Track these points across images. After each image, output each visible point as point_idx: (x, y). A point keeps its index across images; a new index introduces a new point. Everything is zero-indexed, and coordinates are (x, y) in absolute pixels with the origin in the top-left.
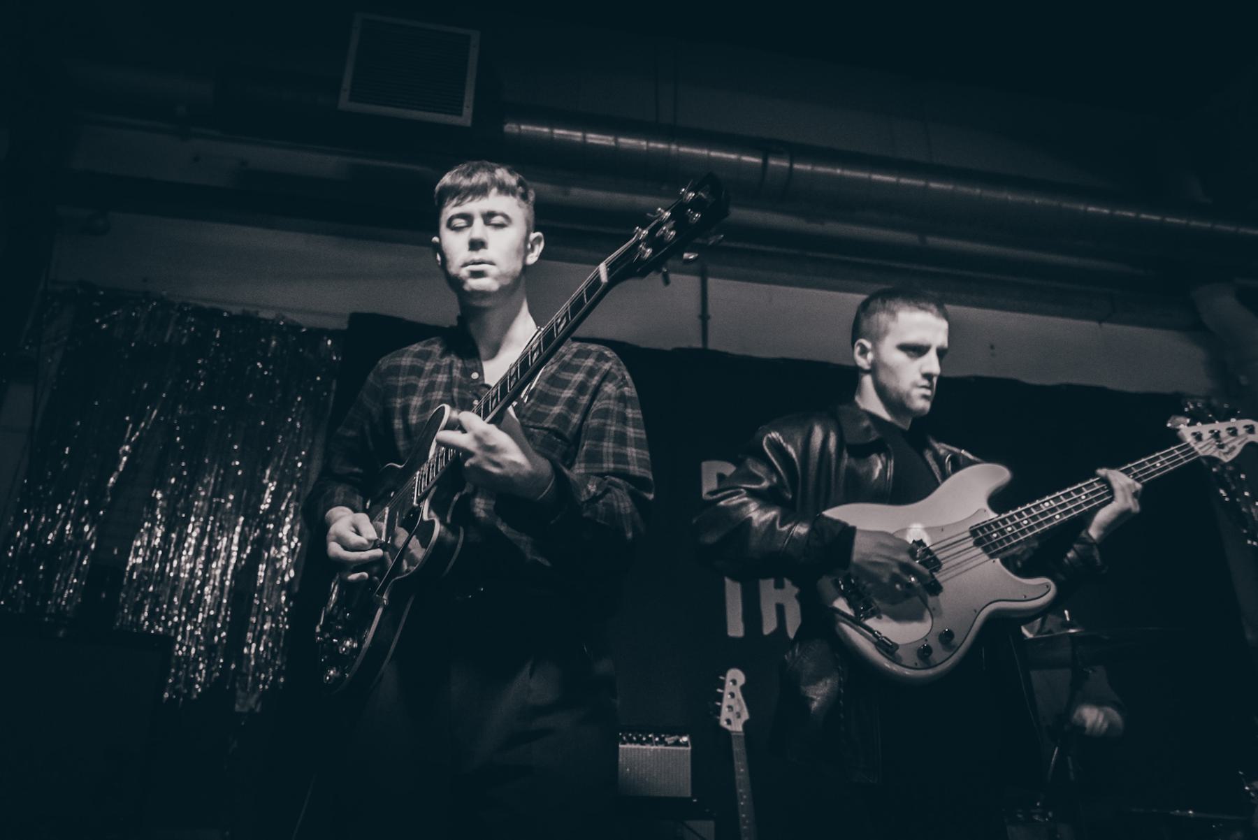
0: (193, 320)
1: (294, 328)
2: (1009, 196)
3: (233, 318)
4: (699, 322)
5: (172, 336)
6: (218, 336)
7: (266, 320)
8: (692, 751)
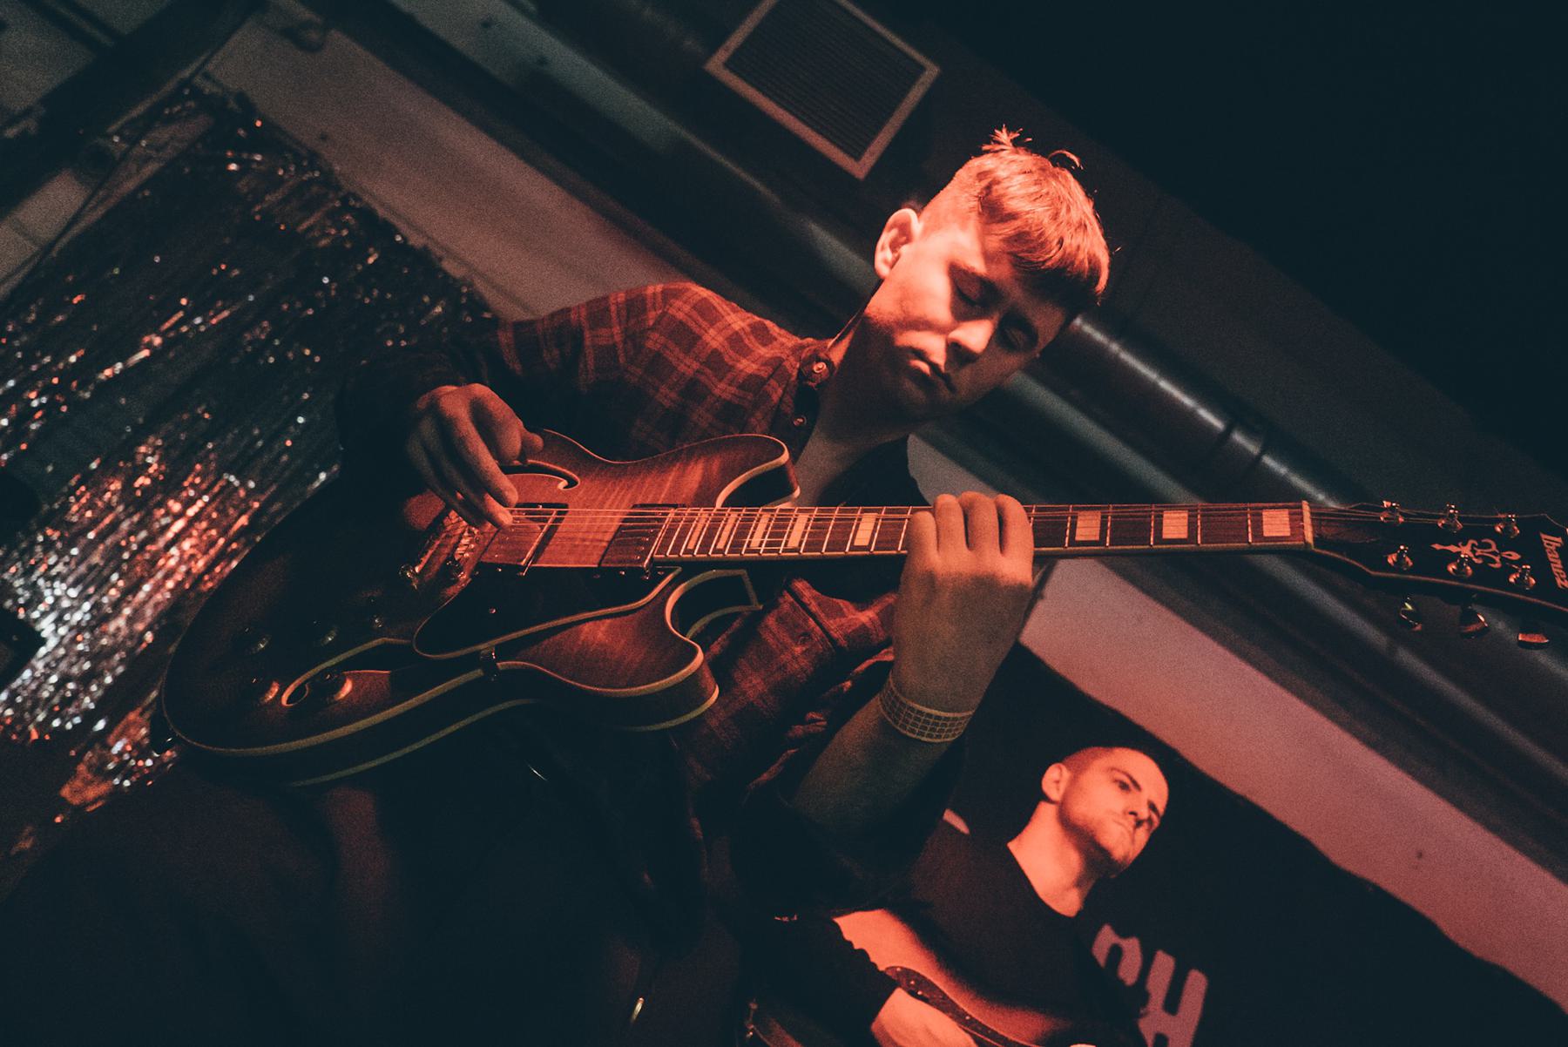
0: (353, 222)
1: (477, 304)
3: (405, 248)
5: (310, 229)
6: (371, 260)
7: (446, 275)
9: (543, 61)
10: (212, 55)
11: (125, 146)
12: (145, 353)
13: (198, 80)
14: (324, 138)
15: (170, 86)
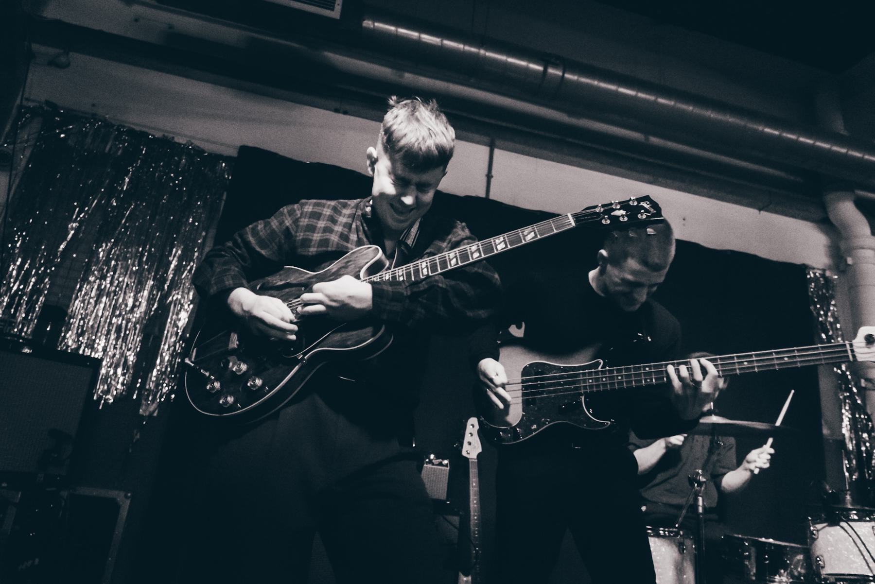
1: (199, 152)
2: (711, 114)
3: (155, 139)
4: (485, 179)
7: (180, 144)
8: (450, 470)
9: (171, 27)
10: (24, 90)
11: (11, 147)
12: (72, 232)
13: (25, 103)
14: (93, 105)
15: (14, 111)
